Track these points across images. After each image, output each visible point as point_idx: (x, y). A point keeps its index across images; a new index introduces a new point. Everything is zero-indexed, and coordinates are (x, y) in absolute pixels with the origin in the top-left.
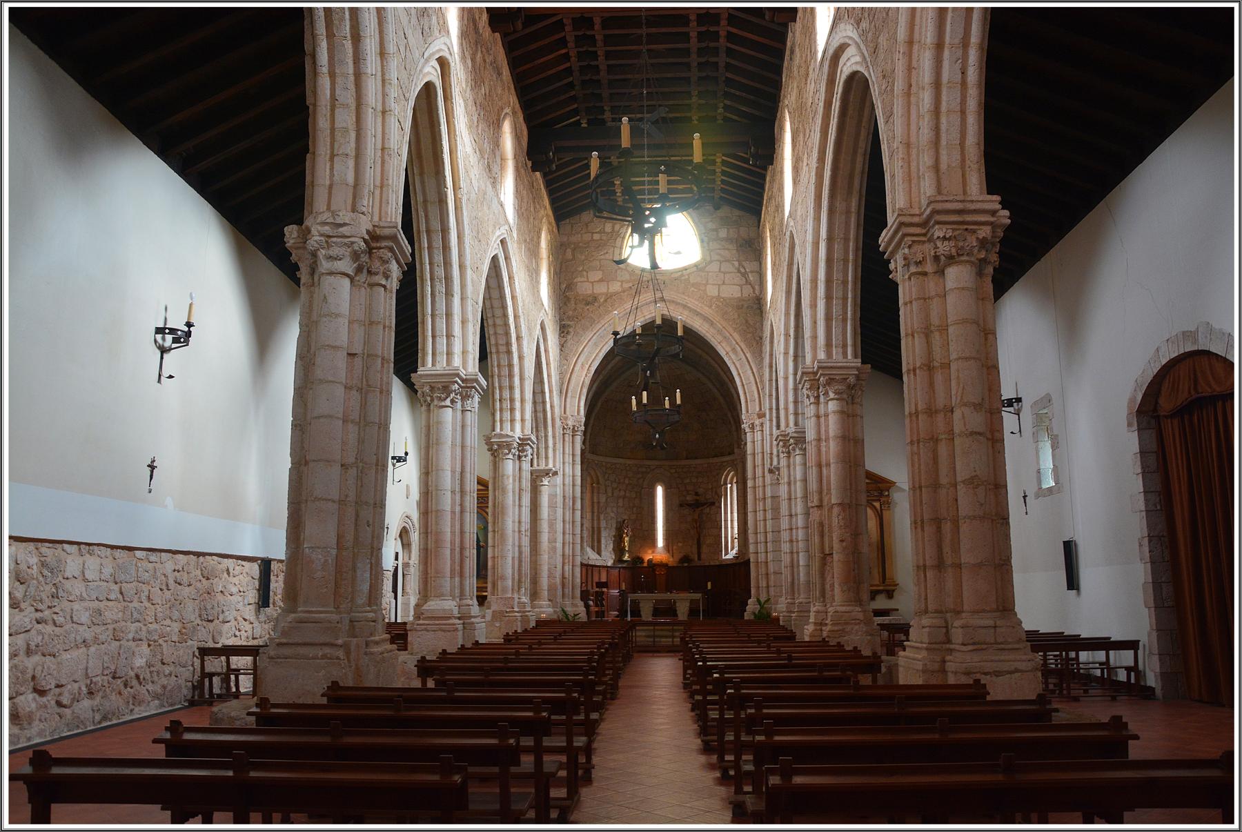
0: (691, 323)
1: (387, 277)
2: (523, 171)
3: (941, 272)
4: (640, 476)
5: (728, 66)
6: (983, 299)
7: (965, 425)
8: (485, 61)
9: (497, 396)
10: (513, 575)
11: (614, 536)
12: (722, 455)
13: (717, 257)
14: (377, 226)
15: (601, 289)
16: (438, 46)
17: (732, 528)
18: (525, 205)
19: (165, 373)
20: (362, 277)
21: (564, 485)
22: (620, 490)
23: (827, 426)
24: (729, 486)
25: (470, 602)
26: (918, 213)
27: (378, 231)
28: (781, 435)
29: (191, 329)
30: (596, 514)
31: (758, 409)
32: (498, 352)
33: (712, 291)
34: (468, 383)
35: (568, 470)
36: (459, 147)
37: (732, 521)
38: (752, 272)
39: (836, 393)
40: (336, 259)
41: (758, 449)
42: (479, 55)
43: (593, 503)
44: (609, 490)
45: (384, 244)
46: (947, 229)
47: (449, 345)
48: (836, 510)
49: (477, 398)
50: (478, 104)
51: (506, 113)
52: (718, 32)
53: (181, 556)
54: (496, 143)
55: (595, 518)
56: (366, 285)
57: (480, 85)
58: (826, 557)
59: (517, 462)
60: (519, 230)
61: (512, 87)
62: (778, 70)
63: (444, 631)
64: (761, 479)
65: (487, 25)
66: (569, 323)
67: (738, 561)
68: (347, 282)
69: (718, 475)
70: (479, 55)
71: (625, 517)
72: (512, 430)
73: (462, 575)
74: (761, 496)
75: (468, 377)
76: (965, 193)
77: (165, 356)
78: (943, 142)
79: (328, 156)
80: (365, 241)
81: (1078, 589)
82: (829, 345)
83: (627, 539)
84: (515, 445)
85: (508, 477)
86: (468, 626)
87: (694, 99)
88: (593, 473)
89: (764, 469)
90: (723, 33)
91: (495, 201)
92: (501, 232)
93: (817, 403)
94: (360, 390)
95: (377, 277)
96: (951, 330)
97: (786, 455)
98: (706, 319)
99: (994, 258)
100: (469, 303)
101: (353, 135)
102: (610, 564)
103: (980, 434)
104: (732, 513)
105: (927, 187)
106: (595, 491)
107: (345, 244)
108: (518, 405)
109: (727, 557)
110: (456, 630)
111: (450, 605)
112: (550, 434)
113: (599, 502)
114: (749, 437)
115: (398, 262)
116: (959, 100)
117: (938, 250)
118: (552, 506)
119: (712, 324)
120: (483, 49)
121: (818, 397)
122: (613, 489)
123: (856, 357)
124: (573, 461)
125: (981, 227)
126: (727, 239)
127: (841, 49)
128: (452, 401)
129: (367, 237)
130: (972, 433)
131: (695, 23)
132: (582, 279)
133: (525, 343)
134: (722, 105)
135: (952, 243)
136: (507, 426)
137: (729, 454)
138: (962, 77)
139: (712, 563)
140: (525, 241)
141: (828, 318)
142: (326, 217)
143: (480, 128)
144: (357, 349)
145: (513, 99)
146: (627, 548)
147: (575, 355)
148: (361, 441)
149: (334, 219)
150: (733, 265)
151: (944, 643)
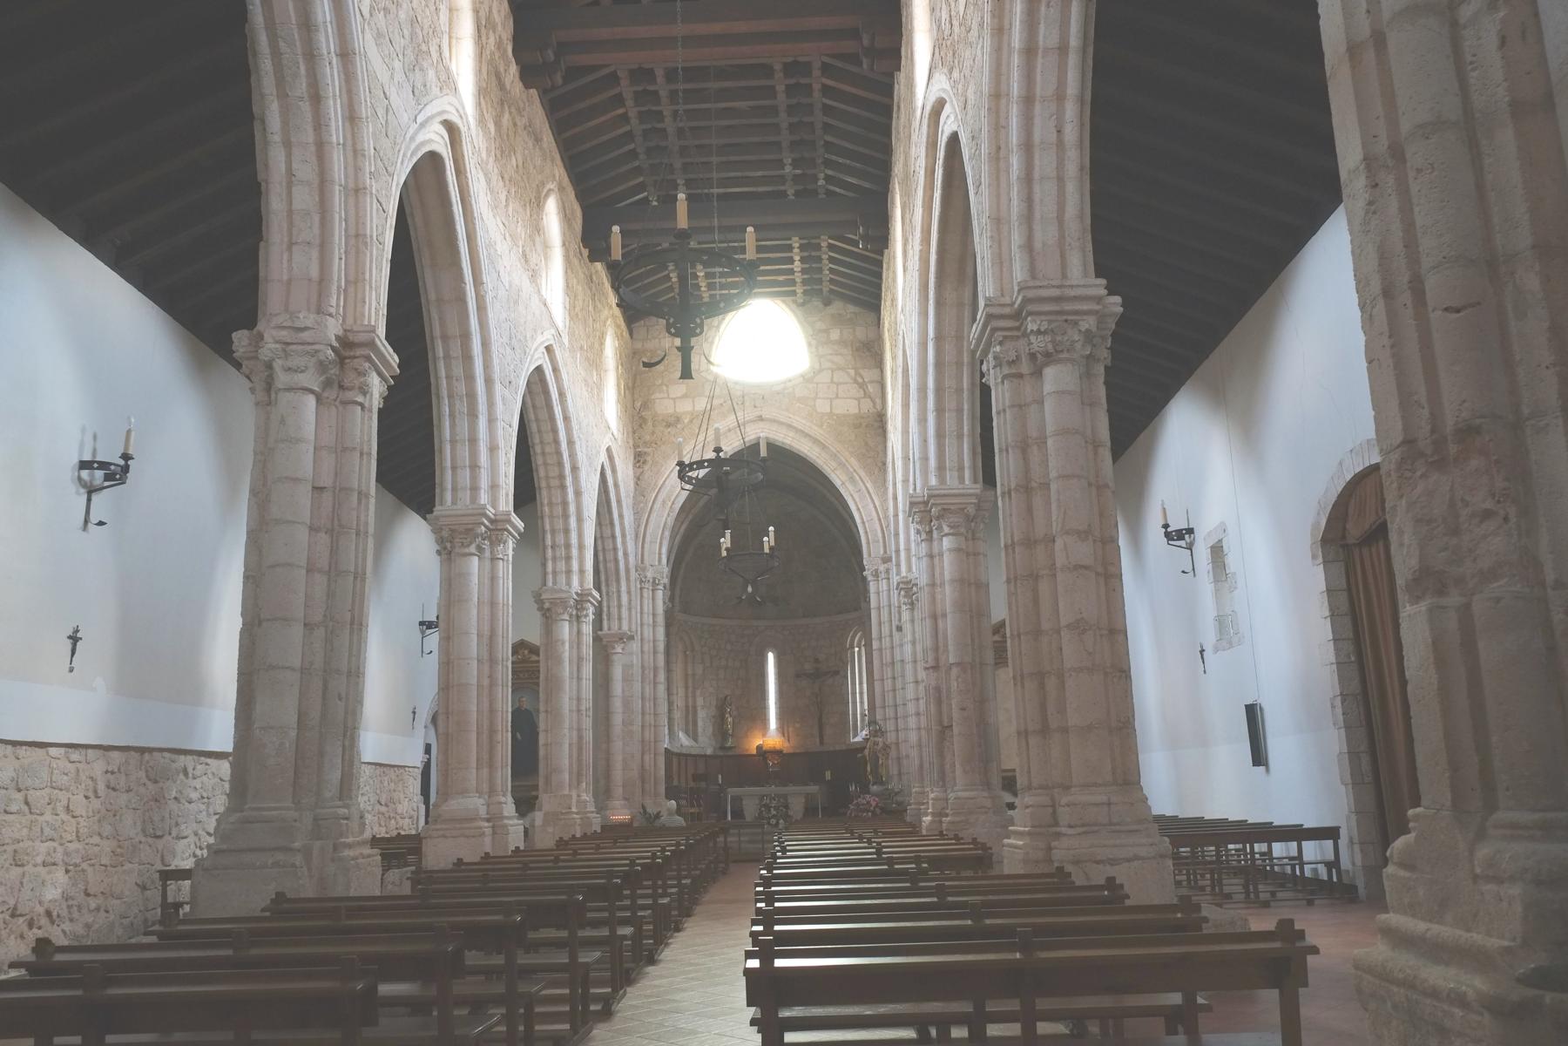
0: (797, 447)
1: (364, 390)
2: (576, 262)
3: (1038, 373)
5: (827, 128)
6: (1090, 405)
7: (1068, 558)
8: (515, 125)
9: (549, 542)
10: (571, 765)
11: (714, 717)
13: (828, 365)
14: (349, 331)
15: (685, 407)
16: (441, 105)
17: (862, 702)
18: (579, 304)
19: (94, 518)
20: (331, 394)
21: (642, 652)
23: (942, 568)
24: (857, 649)
25: (503, 799)
26: (1009, 302)
27: (351, 337)
28: (902, 582)
29: (129, 463)
30: (690, 689)
31: (882, 552)
32: (549, 487)
33: (823, 406)
34: (497, 528)
35: (648, 633)
36: (480, 233)
37: (861, 693)
38: (871, 382)
39: (951, 527)
40: (296, 371)
41: (884, 602)
42: (507, 116)
43: (686, 675)
45: (359, 352)
46: (1042, 321)
47: (475, 478)
48: (955, 671)
49: (511, 544)
50: (506, 176)
51: (550, 190)
52: (811, 85)
53: (115, 754)
54: (537, 228)
55: (690, 695)
56: (337, 403)
57: (510, 156)
58: (944, 730)
59: (575, 623)
60: (571, 334)
61: (558, 157)
62: (887, 131)
63: (467, 837)
64: (888, 639)
65: (517, 79)
66: (646, 450)
68: (311, 401)
70: (506, 117)
72: (569, 584)
73: (491, 766)
74: (889, 660)
75: (498, 517)
76: (1064, 276)
77: (95, 497)
78: (1037, 215)
79: (285, 246)
80: (333, 349)
81: (1266, 764)
82: (941, 468)
84: (572, 602)
85: (563, 643)
86: (498, 829)
87: (788, 169)
89: (891, 625)
90: (817, 87)
91: (535, 299)
92: (547, 337)
93: (930, 539)
94: (330, 532)
95: (351, 393)
96: (1050, 442)
97: (908, 606)
98: (816, 441)
99: (1104, 354)
100: (500, 425)
101: (317, 218)
102: (709, 752)
103: (1086, 568)
104: (861, 683)
105: (1019, 273)
107: (308, 352)
108: (575, 552)
109: (856, 739)
110: (483, 834)
111: (477, 804)
112: (624, 588)
113: (694, 675)
114: (872, 587)
115: (380, 374)
116: (1054, 165)
117: (1031, 346)
118: (627, 679)
119: (824, 447)
120: (513, 110)
121: (930, 532)
123: (975, 481)
124: (654, 622)
125: (1085, 317)
126: (842, 342)
127: (939, 105)
128: (480, 549)
129: (335, 344)
130: (1078, 567)
131: (781, 75)
132: (662, 395)
133: (583, 474)
134: (822, 175)
135: (1048, 338)
136: (562, 579)
137: (856, 610)
138: (1058, 137)
140: (582, 348)
141: (940, 435)
142: (282, 319)
143: (510, 209)
144: (326, 480)
145: (559, 171)
146: (730, 732)
147: (653, 489)
148: (330, 594)
149: (293, 321)
150: (848, 374)
151: (1049, 826)
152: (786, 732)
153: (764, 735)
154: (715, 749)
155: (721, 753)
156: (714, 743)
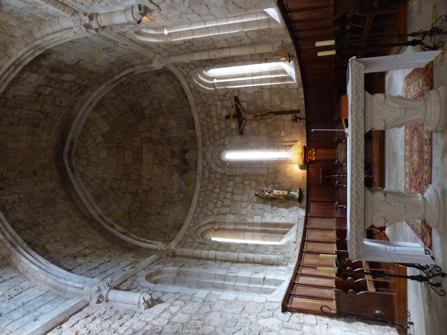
4: (213, 176)
11: (272, 206)
12: (183, 90)
22: (225, 198)
24: (215, 81)
30: (247, 227)
44: (223, 210)
55: (251, 228)
67: (295, 54)
69: (205, 94)
71: (253, 192)
83: (275, 192)
88: (204, 229)
102: (302, 213)
106: (222, 226)
113: (235, 223)
122: (223, 206)
137: (179, 82)
139: (302, 96)
146: (286, 193)
152: (288, 144)
153: (291, 163)
154: (301, 207)
155: (304, 202)
156: (296, 208)
